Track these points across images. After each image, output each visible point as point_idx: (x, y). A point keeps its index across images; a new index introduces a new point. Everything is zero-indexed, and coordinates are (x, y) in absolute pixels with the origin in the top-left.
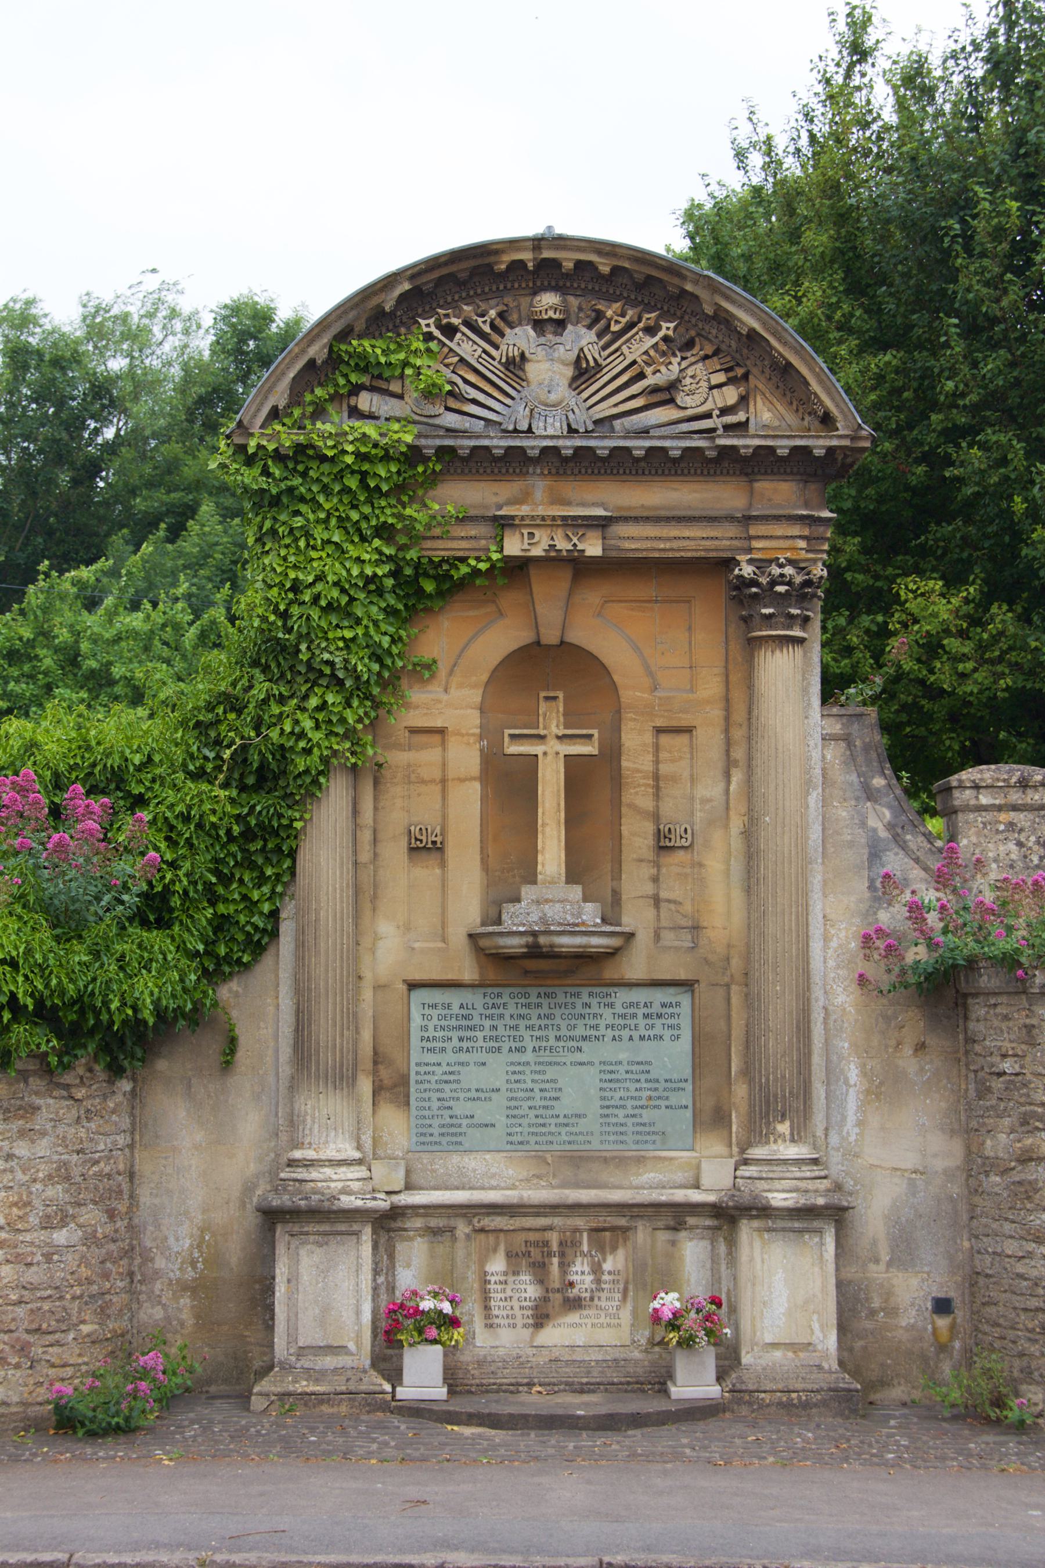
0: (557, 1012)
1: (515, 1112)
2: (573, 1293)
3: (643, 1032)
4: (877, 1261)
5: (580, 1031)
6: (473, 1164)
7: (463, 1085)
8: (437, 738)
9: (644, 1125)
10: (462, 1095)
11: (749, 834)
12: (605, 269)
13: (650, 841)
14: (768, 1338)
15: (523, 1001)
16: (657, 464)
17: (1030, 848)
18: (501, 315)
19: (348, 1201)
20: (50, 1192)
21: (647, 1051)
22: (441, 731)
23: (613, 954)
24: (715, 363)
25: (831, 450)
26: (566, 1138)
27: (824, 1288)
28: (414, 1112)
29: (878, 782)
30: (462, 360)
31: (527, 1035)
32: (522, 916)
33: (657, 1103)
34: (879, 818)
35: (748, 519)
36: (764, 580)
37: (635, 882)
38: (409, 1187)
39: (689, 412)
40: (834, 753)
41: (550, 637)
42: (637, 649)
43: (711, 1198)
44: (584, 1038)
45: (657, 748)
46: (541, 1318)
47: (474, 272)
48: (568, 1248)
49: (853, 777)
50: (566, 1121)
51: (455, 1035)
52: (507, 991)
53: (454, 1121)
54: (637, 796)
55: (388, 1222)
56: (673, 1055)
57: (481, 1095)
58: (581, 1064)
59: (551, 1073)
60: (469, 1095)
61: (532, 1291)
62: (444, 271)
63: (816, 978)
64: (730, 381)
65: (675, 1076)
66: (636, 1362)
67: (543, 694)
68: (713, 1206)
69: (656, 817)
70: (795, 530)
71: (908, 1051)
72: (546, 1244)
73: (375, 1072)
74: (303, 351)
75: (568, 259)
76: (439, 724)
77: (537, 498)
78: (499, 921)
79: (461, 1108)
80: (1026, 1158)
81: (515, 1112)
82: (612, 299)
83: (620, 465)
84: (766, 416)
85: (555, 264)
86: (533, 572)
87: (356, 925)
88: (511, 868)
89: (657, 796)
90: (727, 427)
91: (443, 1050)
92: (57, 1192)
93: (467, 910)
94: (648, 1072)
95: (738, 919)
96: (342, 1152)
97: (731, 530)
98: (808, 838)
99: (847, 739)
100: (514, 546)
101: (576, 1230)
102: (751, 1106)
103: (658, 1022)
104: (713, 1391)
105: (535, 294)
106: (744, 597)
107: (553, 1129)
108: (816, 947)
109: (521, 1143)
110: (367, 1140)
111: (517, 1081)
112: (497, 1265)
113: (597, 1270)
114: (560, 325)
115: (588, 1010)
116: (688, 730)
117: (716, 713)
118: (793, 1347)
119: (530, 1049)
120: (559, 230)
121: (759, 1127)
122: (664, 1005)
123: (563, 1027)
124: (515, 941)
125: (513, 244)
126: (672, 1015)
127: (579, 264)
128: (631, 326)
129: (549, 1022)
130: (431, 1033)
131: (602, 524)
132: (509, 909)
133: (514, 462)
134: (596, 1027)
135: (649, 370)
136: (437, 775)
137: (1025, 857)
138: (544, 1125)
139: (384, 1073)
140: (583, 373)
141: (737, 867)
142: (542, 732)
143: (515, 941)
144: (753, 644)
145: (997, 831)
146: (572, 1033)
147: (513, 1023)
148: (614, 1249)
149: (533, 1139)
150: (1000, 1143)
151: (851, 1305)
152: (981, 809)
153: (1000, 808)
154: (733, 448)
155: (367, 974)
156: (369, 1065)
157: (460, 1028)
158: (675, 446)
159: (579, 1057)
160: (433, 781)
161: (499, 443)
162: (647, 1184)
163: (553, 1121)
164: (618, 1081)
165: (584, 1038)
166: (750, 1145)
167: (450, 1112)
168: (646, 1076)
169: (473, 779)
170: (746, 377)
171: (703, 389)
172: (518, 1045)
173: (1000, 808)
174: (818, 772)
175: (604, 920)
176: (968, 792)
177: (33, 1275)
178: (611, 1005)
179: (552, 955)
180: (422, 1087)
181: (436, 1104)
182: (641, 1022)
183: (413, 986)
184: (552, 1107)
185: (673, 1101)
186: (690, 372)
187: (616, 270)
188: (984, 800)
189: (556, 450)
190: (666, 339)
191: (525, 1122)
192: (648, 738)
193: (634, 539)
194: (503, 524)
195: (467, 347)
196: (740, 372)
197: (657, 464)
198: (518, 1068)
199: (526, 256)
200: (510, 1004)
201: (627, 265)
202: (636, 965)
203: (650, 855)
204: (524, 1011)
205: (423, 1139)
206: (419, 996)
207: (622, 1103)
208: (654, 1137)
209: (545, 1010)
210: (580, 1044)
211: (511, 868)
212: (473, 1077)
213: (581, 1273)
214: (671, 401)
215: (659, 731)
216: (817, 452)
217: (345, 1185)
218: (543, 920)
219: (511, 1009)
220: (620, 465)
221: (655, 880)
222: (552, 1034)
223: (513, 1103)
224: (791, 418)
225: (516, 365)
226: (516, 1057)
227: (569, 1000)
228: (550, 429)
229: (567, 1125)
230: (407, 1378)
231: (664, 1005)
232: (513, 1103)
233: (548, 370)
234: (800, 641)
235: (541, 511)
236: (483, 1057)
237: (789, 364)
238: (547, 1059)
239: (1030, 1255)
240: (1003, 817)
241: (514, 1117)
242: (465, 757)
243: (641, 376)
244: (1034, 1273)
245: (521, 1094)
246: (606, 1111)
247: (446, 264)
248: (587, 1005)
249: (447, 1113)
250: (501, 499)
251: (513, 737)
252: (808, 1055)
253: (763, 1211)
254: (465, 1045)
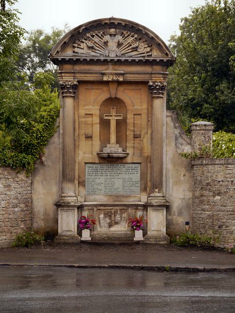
2: (117, 221)
4: (175, 215)
5: (118, 172)
6: (97, 197)
8: (91, 116)
11: (151, 135)
12: (124, 24)
13: (133, 136)
14: (153, 229)
16: (133, 63)
18: (103, 33)
19: (72, 204)
20: (14, 201)
21: (131, 176)
22: (92, 114)
23: (125, 157)
24: (146, 43)
25: (168, 60)
27: (163, 220)
28: (86, 187)
29: (177, 125)
32: (107, 150)
34: (177, 132)
35: (151, 74)
36: (154, 86)
37: (130, 144)
38: (85, 201)
39: (140, 53)
40: (169, 119)
41: (113, 96)
42: (131, 100)
43: (143, 203)
45: (134, 118)
46: (110, 225)
47: (97, 25)
48: (115, 213)
49: (172, 124)
54: (130, 127)
55: (80, 208)
56: (136, 177)
57: (99, 184)
59: (113, 180)
61: (108, 221)
62: (92, 24)
63: (164, 162)
64: (149, 46)
66: (128, 234)
68: (143, 205)
69: (134, 131)
70: (161, 76)
71: (182, 176)
72: (111, 212)
74: (63, 40)
75: (116, 22)
76: (91, 113)
77: (110, 69)
78: (102, 151)
79: (95, 187)
80: (202, 196)
82: (125, 30)
83: (126, 63)
84: (155, 54)
85: (114, 23)
86: (110, 83)
87: (74, 151)
88: (105, 141)
89: (134, 127)
90: (147, 56)
92: (15, 201)
93: (97, 149)
95: (149, 151)
96: (71, 194)
97: (148, 76)
98: (163, 136)
99: (171, 116)
100: (105, 79)
101: (117, 209)
102: (151, 186)
103: (134, 171)
104: (142, 239)
105: (110, 29)
106: (151, 89)
108: (164, 156)
110: (77, 192)
112: (102, 216)
113: (121, 217)
114: (115, 35)
116: (140, 115)
117: (146, 111)
118: (158, 231)
120: (114, 17)
121: (152, 191)
124: (105, 155)
125: (106, 19)
127: (118, 23)
128: (129, 35)
131: (123, 74)
132: (104, 148)
133: (105, 62)
135: (132, 44)
136: (91, 123)
139: (80, 180)
140: (119, 45)
141: (149, 141)
143: (105, 155)
144: (153, 98)
148: (124, 213)
150: (197, 194)
151: (169, 224)
152: (197, 130)
153: (200, 130)
154: (149, 60)
155: (77, 161)
156: (77, 178)
158: (137, 59)
159: (118, 177)
160: (90, 124)
161: (102, 58)
162: (131, 201)
166: (151, 194)
169: (97, 124)
170: (152, 46)
171: (143, 48)
173: (200, 130)
174: (165, 123)
175: (123, 151)
177: (10, 216)
179: (113, 158)
181: (90, 186)
183: (86, 163)
185: (137, 185)
186: (141, 45)
187: (125, 24)
188: (198, 128)
189: (113, 60)
190: (136, 38)
192: (132, 116)
193: (130, 78)
194: (103, 74)
195: (96, 39)
196: (150, 45)
197: (133, 63)
199: (107, 21)
200: (105, 166)
201: (127, 23)
202: (129, 159)
203: (133, 139)
206: (87, 165)
211: (105, 141)
212: (98, 181)
213: (118, 218)
214: (137, 50)
215: (135, 115)
216: (165, 61)
217: (71, 200)
218: (111, 151)
220: (126, 63)
221: (134, 143)
224: (160, 54)
225: (106, 43)
226: (106, 177)
228: (112, 56)
230: (83, 236)
233: (113, 44)
234: (162, 97)
235: (110, 72)
236: (99, 177)
237: (159, 44)
239: (202, 214)
240: (201, 131)
242: (96, 120)
243: (131, 45)
244: (202, 217)
250: (103, 69)
252: (162, 177)
253: (152, 206)
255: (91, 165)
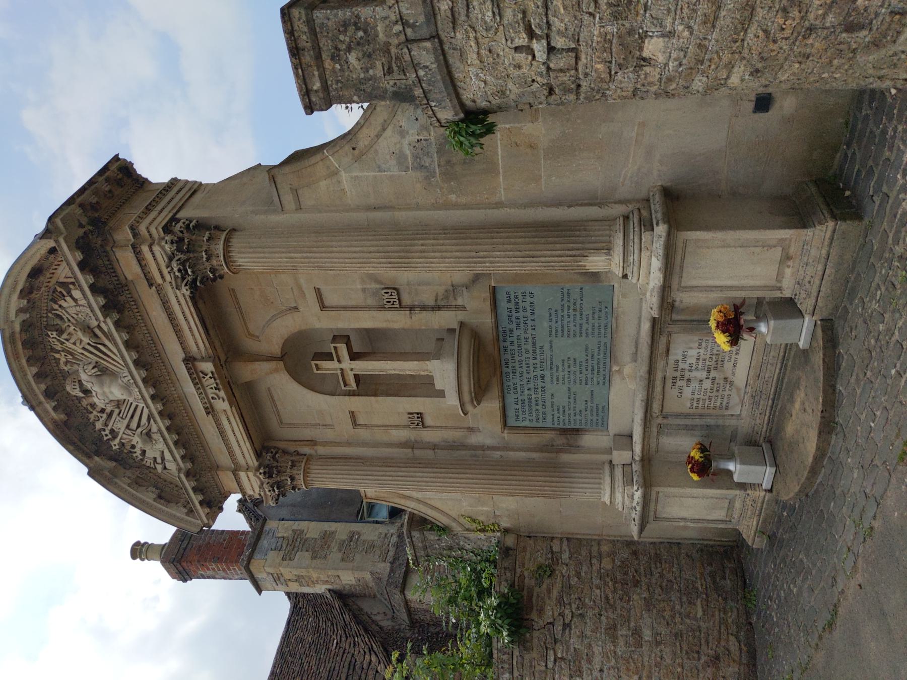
0: (517, 359)
1: (584, 380)
3: (528, 313)
5: (529, 347)
7: (566, 404)
9: (594, 313)
10: (572, 406)
15: (511, 376)
17: (351, 37)
26: (602, 356)
30: (128, 427)
31: (532, 374)
33: (578, 306)
44: (534, 344)
50: (590, 356)
51: (534, 407)
52: (505, 370)
53: (589, 409)
58: (551, 347)
60: (572, 402)
65: (559, 295)
67: (315, 371)
73: (559, 451)
75: (39, 389)
79: (581, 406)
81: (584, 380)
91: (544, 413)
94: (556, 311)
103: (521, 304)
107: (595, 362)
109: (604, 378)
111: (563, 379)
115: (515, 343)
119: (542, 373)
122: (509, 301)
123: (527, 356)
126: (516, 297)
129: (524, 363)
130: (534, 418)
134: (526, 339)
137: (358, 44)
138: (593, 367)
142: (339, 372)
145: (342, 70)
146: (531, 351)
147: (525, 380)
149: (602, 372)
157: (530, 405)
159: (547, 347)
163: (590, 362)
164: (563, 327)
165: (534, 344)
167: (583, 411)
168: (559, 312)
172: (539, 378)
176: (314, 99)
178: (511, 331)
180: (567, 421)
181: (578, 417)
182: (521, 314)
184: (581, 362)
185: (575, 295)
188: (317, 85)
191: (590, 376)
198: (555, 379)
204: (518, 375)
205: (600, 424)
207: (578, 326)
208: (603, 308)
209: (517, 365)
210: (538, 347)
212: (561, 399)
219: (517, 381)
222: (532, 362)
223: (578, 381)
227: (509, 352)
229: (593, 355)
231: (509, 301)
232: (578, 381)
236: (548, 396)
238: (549, 364)
240: (328, 64)
241: (586, 381)
245: (572, 377)
246: (584, 335)
247: (73, 444)
248: (512, 343)
249: (584, 413)
251: (345, 385)
254: (540, 403)
255: (511, 413)
